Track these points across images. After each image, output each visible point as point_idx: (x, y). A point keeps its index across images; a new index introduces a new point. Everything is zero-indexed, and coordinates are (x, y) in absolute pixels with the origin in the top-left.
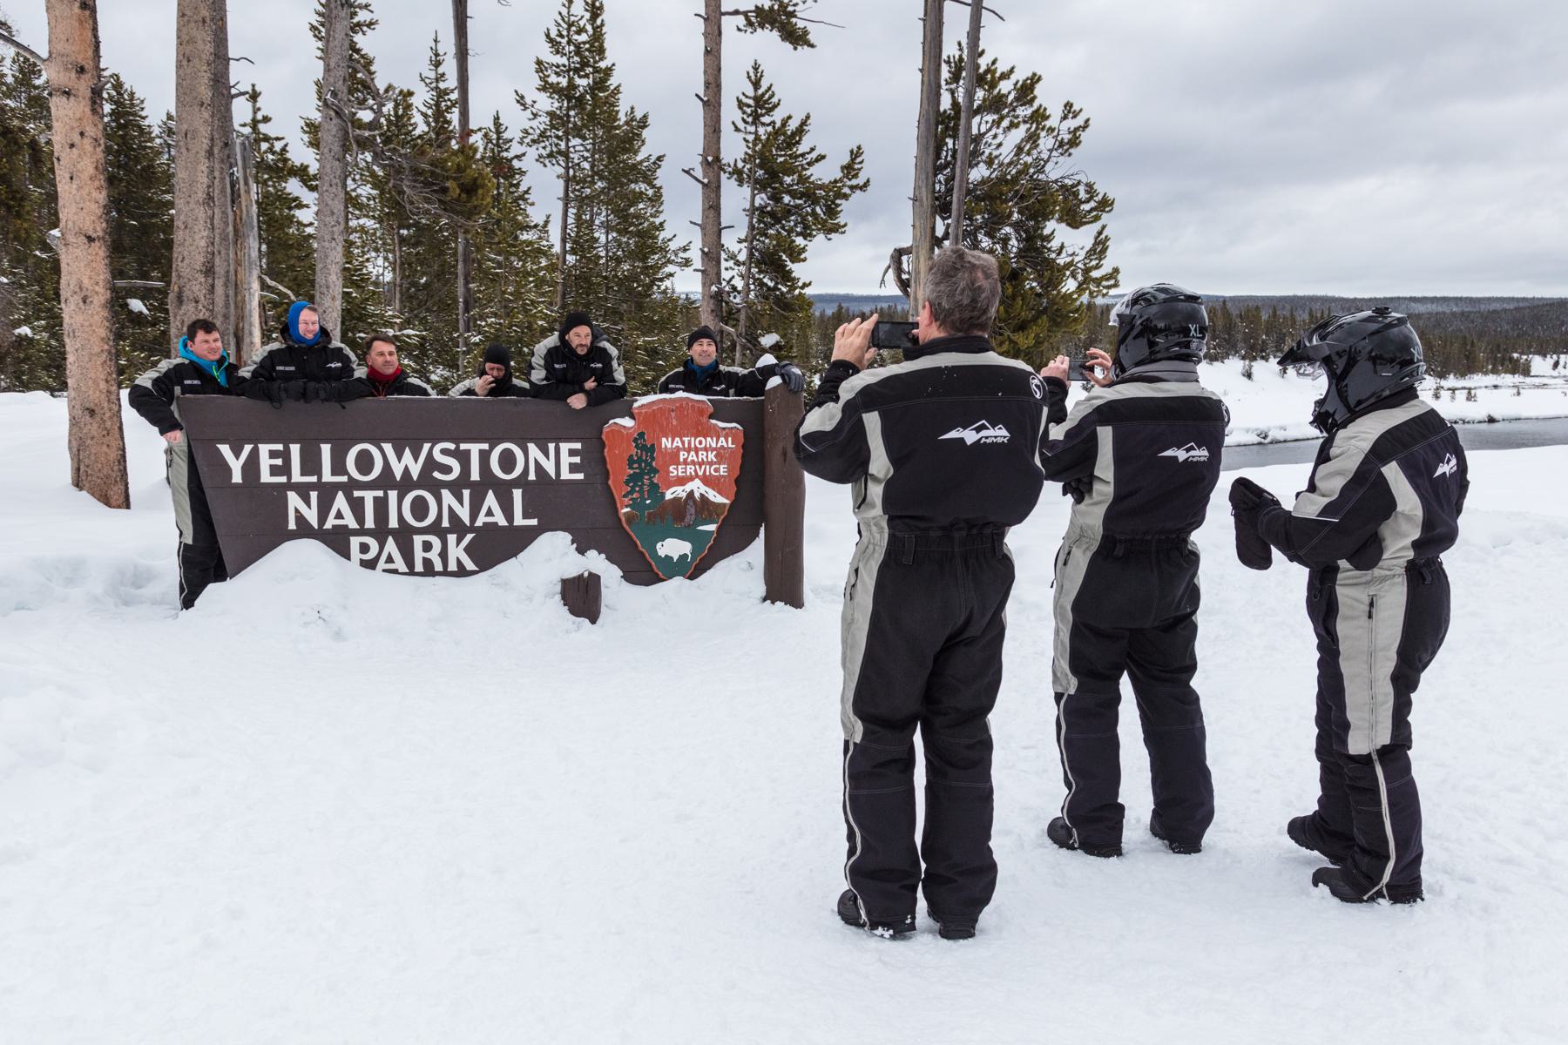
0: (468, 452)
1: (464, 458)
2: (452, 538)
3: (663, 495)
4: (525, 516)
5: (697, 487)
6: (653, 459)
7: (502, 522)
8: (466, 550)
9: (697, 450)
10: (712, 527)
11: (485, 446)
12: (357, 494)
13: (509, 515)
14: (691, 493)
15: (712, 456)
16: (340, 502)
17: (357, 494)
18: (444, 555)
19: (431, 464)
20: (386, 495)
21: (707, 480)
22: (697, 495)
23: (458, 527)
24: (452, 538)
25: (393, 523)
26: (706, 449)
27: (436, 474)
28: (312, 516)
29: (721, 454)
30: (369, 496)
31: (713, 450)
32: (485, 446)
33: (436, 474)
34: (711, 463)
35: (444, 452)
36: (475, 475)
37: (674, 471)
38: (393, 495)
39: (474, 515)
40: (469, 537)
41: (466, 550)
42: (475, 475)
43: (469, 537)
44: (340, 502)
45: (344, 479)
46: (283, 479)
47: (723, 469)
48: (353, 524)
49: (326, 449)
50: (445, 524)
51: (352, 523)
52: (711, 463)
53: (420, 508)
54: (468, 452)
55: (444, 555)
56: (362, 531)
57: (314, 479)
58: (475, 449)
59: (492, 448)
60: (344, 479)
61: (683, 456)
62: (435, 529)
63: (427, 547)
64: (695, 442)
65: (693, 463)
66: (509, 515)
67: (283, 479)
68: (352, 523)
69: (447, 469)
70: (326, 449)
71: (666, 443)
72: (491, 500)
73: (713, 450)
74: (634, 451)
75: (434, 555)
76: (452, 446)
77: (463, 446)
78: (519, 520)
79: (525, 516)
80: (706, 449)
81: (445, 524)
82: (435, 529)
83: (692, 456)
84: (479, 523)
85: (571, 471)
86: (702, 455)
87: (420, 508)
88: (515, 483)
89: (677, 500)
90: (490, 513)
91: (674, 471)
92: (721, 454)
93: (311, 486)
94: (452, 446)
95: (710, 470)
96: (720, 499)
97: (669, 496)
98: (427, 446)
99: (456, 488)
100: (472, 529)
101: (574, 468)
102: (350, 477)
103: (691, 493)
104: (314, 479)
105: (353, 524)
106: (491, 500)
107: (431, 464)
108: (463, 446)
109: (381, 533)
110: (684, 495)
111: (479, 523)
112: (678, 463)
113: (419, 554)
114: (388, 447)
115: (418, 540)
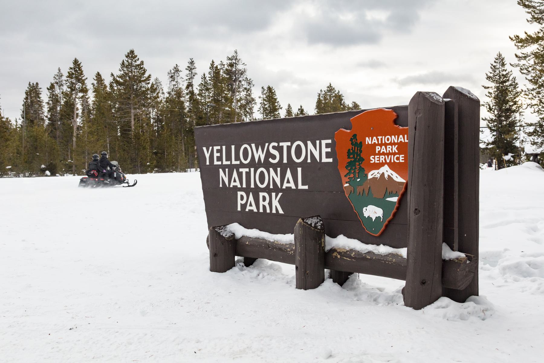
0: (283, 146)
1: (280, 149)
2: (274, 194)
3: (366, 176)
4: (303, 184)
5: (386, 170)
6: (361, 151)
7: (294, 187)
8: (279, 201)
9: (386, 145)
10: (395, 199)
11: (289, 144)
12: (241, 170)
13: (296, 184)
14: (383, 173)
15: (395, 149)
16: (235, 175)
17: (241, 170)
18: (270, 204)
19: (269, 155)
20: (250, 170)
21: (393, 166)
22: (386, 176)
23: (276, 189)
24: (274, 194)
25: (252, 186)
26: (391, 144)
27: (270, 160)
28: (226, 180)
29: (402, 147)
30: (244, 170)
31: (394, 144)
32: (289, 144)
33: (270, 160)
34: (394, 154)
35: (274, 147)
36: (285, 161)
37: (374, 159)
38: (252, 170)
39: (282, 183)
40: (280, 194)
41: (279, 201)
42: (285, 161)
43: (280, 194)
44: (235, 175)
45: (238, 162)
46: (220, 163)
47: (402, 157)
48: (239, 186)
49: (233, 147)
50: (271, 187)
51: (238, 184)
52: (394, 154)
53: (262, 178)
54: (283, 146)
55: (270, 204)
56: (241, 189)
57: (229, 163)
58: (285, 145)
59: (292, 144)
60: (238, 162)
61: (378, 149)
62: (267, 190)
63: (264, 199)
64: (385, 139)
65: (383, 154)
66: (296, 184)
67: (220, 163)
68: (238, 184)
69: (274, 157)
70: (233, 147)
71: (368, 141)
72: (289, 174)
73: (394, 144)
74: (350, 147)
75: (266, 203)
76: (276, 144)
77: (281, 144)
78: (300, 187)
79: (303, 185)
80: (391, 144)
81: (271, 187)
82: (267, 190)
83: (383, 150)
84: (284, 187)
85: (327, 157)
86: (389, 148)
87: (262, 178)
88: (300, 165)
89: (374, 179)
90: (288, 182)
91: (374, 159)
92: (402, 147)
93: (227, 166)
94: (276, 144)
95: (394, 159)
96: (399, 179)
97: (370, 177)
98: (267, 144)
99: (275, 167)
100: (281, 190)
101: (327, 157)
102: (241, 162)
103: (383, 173)
104: (229, 163)
105: (239, 186)
106: (289, 174)
107: (269, 155)
108: (281, 144)
109: (247, 190)
110: (378, 176)
111: (284, 187)
112: (375, 154)
113: (261, 203)
114: (253, 145)
115: (261, 194)
